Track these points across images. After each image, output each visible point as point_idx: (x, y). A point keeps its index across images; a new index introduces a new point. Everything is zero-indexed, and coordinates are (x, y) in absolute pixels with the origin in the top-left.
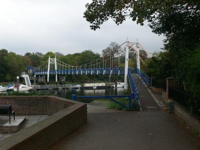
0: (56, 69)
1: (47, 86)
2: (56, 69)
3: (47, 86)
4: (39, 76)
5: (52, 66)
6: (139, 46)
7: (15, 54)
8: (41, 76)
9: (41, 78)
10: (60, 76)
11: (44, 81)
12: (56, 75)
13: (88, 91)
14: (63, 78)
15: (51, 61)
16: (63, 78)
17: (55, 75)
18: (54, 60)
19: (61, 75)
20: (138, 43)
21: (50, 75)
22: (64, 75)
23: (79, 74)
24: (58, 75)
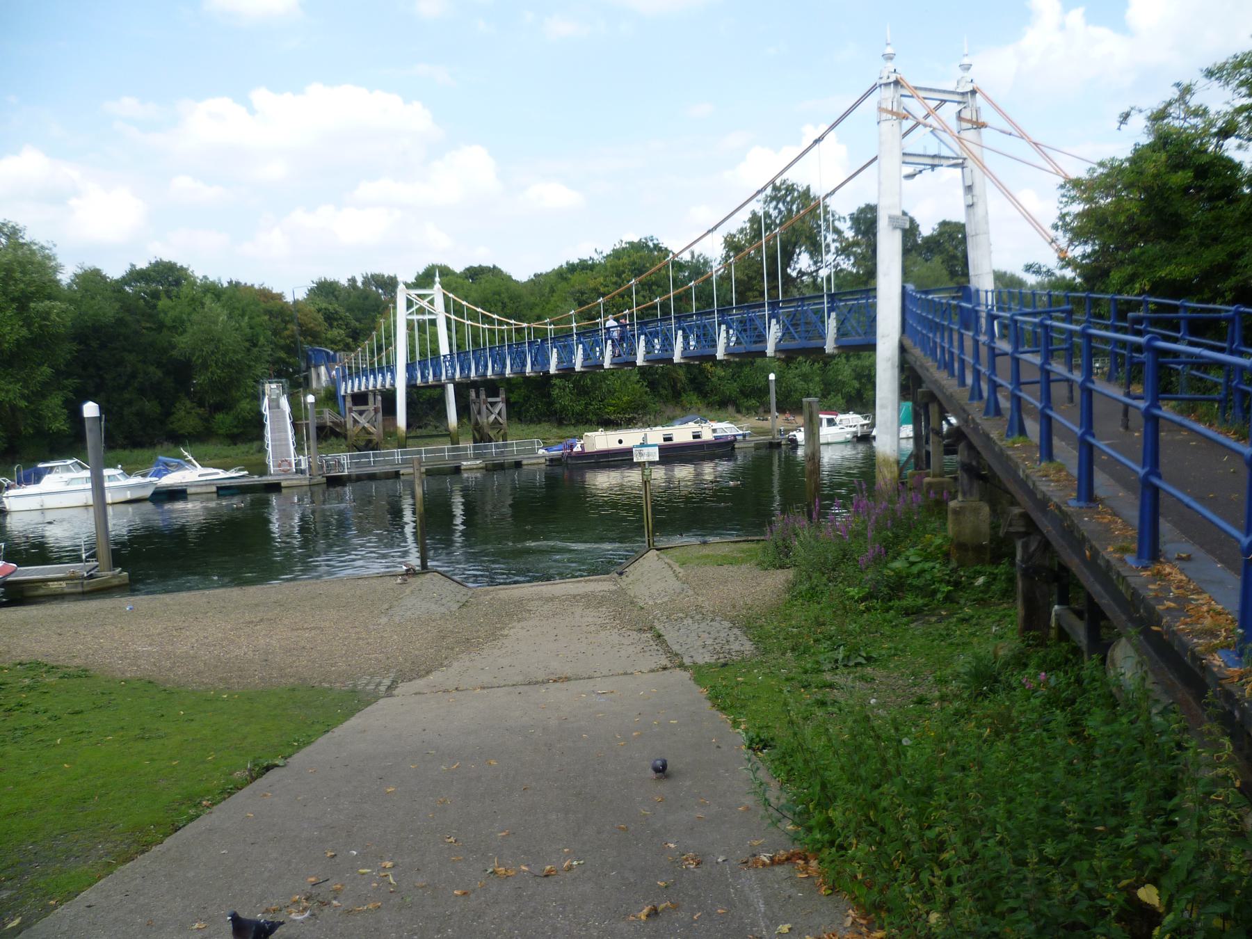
0: (444, 349)
1: (395, 457)
2: (444, 349)
3: (395, 457)
4: (349, 399)
5: (423, 330)
6: (987, 115)
7: (175, 264)
8: (360, 399)
9: (361, 413)
10: (473, 394)
11: (376, 431)
12: (450, 388)
13: (603, 481)
14: (493, 404)
15: (410, 304)
16: (493, 404)
18: (431, 302)
19: (474, 384)
20: (973, 92)
21: (411, 387)
22: (491, 388)
23: (566, 372)
24: (462, 390)
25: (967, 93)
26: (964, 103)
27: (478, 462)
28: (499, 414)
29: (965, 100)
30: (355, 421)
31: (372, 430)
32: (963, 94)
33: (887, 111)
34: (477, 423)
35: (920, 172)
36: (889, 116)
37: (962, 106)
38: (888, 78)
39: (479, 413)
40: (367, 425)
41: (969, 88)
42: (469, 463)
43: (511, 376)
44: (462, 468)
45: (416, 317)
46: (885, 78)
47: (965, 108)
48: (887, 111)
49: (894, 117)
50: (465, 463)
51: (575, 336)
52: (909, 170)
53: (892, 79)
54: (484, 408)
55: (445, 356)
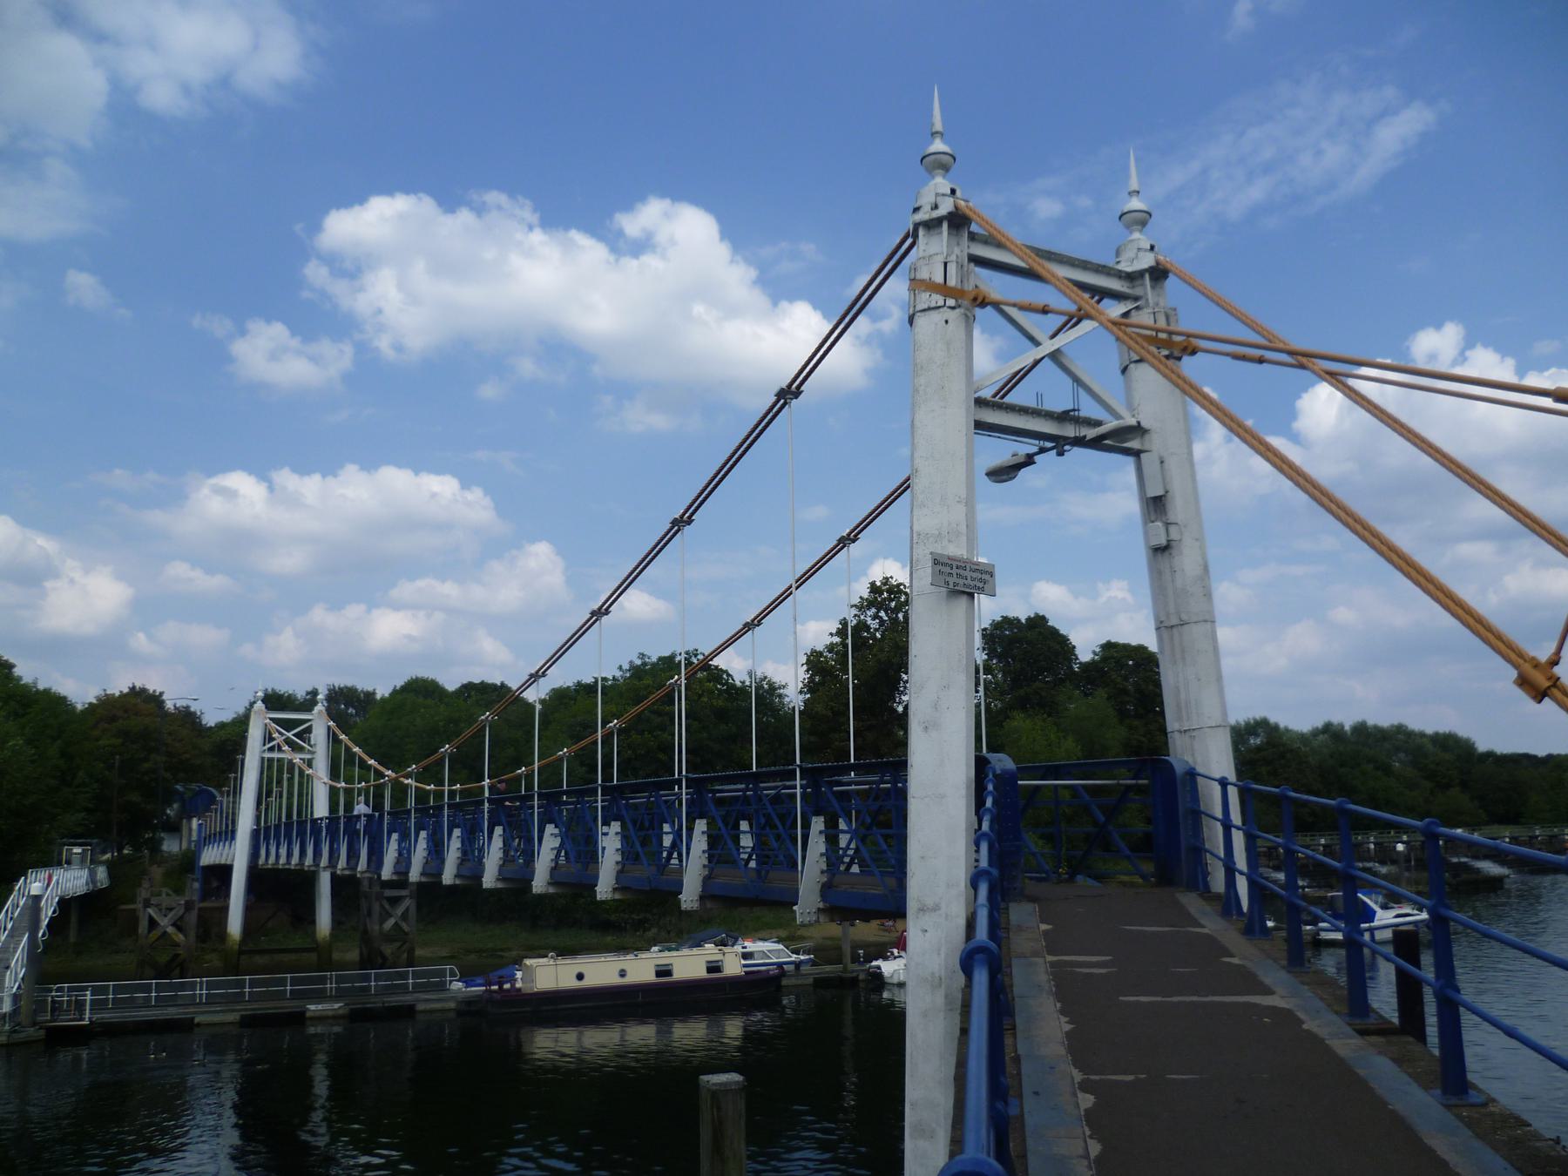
15: (268, 737)
20: (1158, 274)
26: (1136, 299)
27: (336, 1006)
28: (404, 917)
29: (1138, 291)
30: (153, 923)
31: (180, 938)
32: (1131, 277)
33: (931, 287)
34: (365, 932)
35: (1029, 460)
36: (938, 299)
37: (1129, 305)
38: (936, 207)
39: (369, 914)
40: (170, 930)
41: (1147, 261)
42: (320, 1007)
43: (347, 872)
44: (308, 1014)
45: (267, 755)
46: (927, 208)
47: (1137, 308)
48: (931, 287)
49: (951, 302)
50: (312, 1007)
51: (487, 805)
52: (1003, 451)
53: (946, 207)
54: (376, 907)
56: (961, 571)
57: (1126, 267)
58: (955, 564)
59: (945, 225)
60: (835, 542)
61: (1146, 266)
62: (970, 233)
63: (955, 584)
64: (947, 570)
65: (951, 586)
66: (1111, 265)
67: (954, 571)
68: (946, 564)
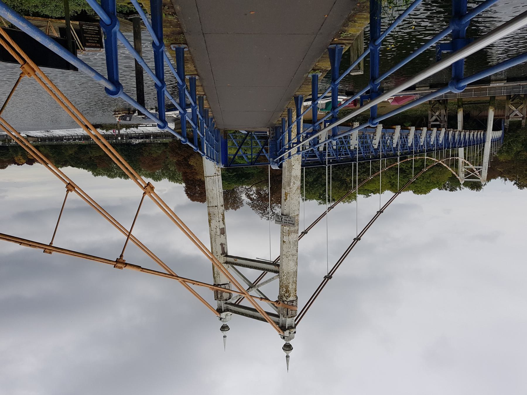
6: (209, 294)
17: (465, 128)
20: (220, 311)
21: (485, 129)
25: (224, 311)
26: (226, 303)
29: (226, 305)
32: (227, 310)
37: (228, 301)
41: (223, 315)
45: (481, 167)
55: (460, 147)
56: (286, 221)
57: (229, 313)
58: (288, 224)
59: (287, 327)
60: (308, 232)
61: (223, 313)
62: (279, 325)
63: (288, 218)
64: (290, 222)
65: (289, 217)
66: (233, 313)
67: (288, 222)
68: (290, 224)
